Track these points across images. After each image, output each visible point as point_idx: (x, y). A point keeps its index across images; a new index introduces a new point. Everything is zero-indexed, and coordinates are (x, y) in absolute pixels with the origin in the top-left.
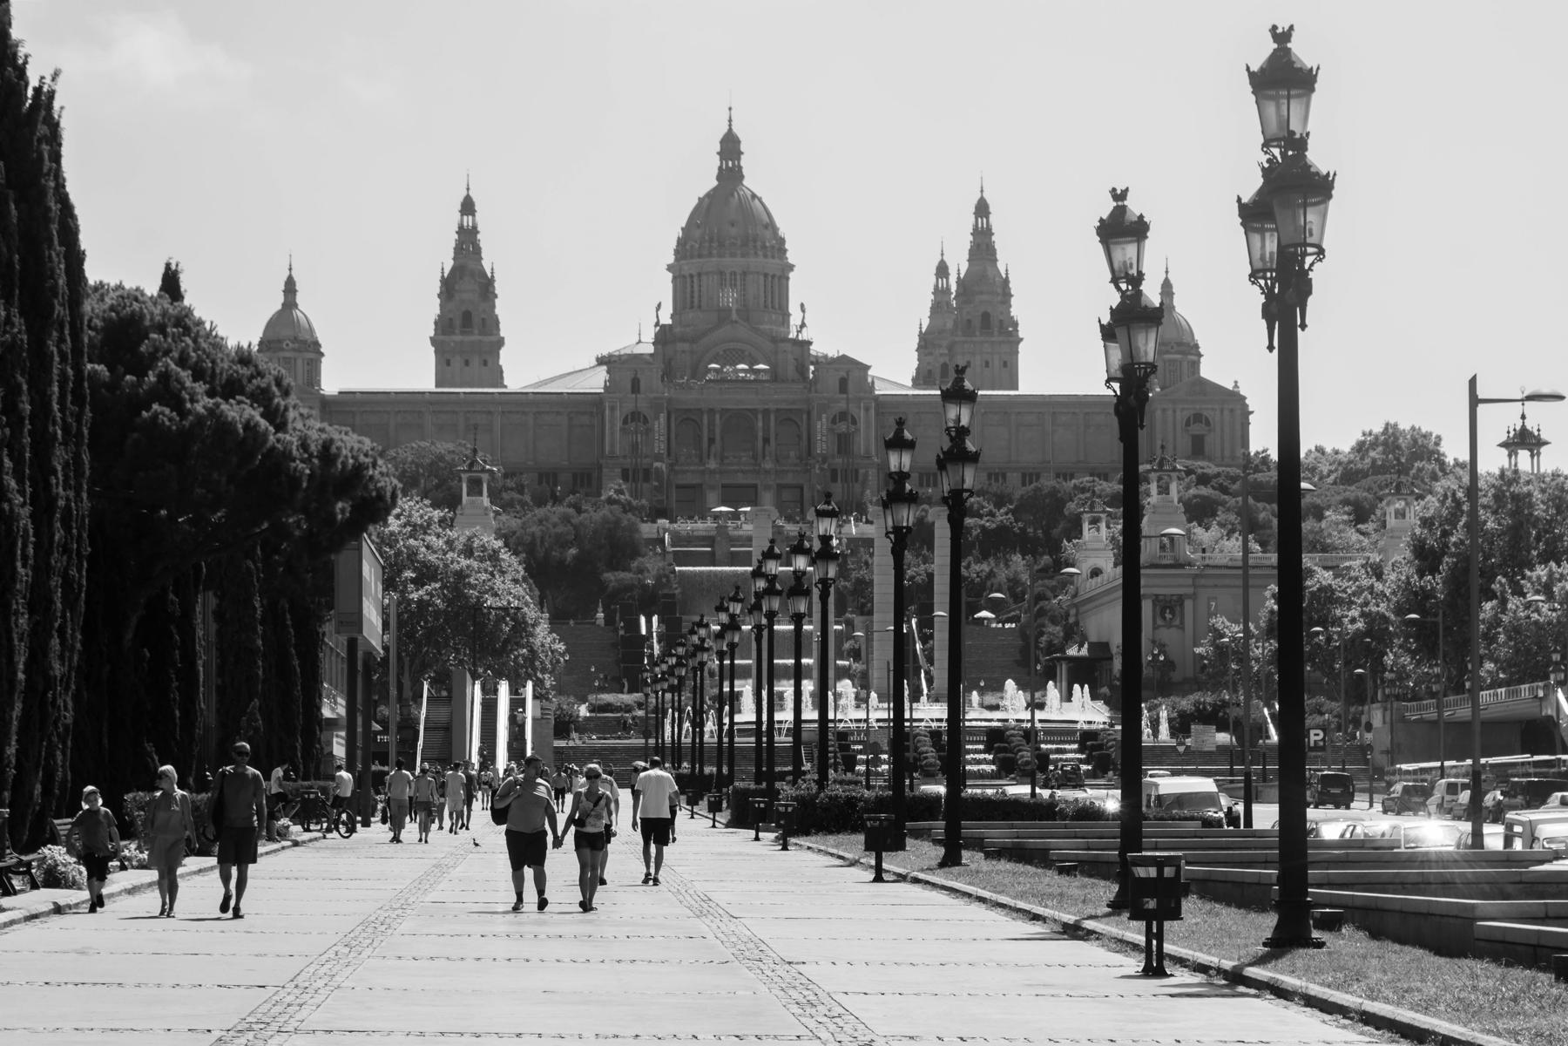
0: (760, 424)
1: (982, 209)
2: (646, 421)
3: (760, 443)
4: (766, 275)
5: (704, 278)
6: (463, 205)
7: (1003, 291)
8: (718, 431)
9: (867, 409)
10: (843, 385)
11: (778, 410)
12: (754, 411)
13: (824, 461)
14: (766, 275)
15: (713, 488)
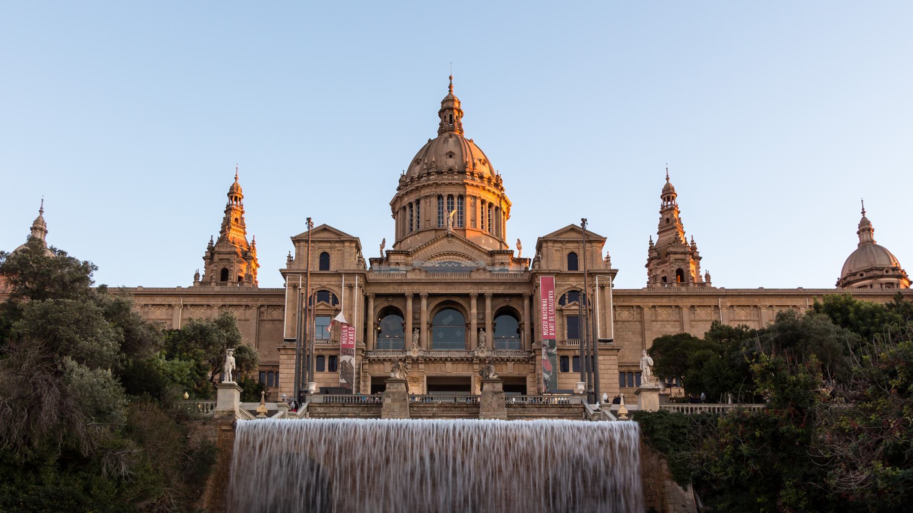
0: (474, 311)
1: (668, 194)
2: (336, 301)
3: (474, 333)
4: (483, 202)
5: (422, 202)
6: (232, 188)
7: (693, 253)
8: (425, 318)
9: (602, 287)
10: (573, 259)
11: (495, 296)
12: (467, 296)
13: (552, 344)
14: (483, 202)
15: (415, 380)
